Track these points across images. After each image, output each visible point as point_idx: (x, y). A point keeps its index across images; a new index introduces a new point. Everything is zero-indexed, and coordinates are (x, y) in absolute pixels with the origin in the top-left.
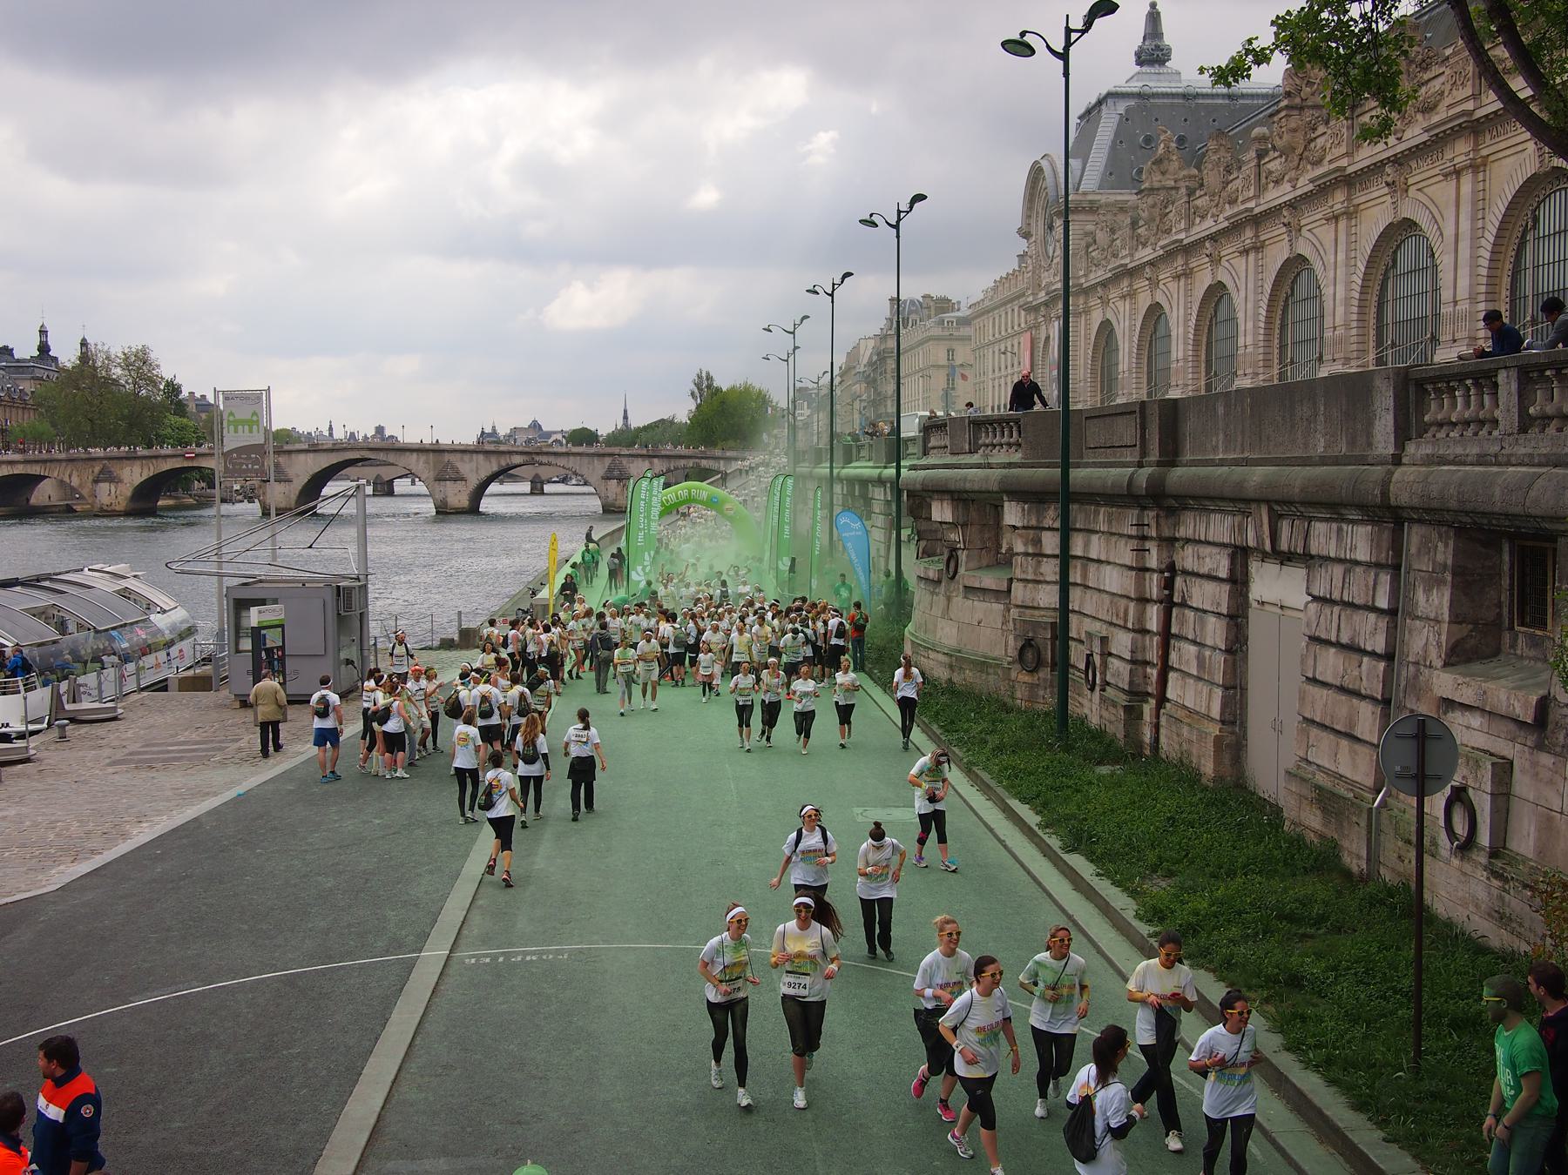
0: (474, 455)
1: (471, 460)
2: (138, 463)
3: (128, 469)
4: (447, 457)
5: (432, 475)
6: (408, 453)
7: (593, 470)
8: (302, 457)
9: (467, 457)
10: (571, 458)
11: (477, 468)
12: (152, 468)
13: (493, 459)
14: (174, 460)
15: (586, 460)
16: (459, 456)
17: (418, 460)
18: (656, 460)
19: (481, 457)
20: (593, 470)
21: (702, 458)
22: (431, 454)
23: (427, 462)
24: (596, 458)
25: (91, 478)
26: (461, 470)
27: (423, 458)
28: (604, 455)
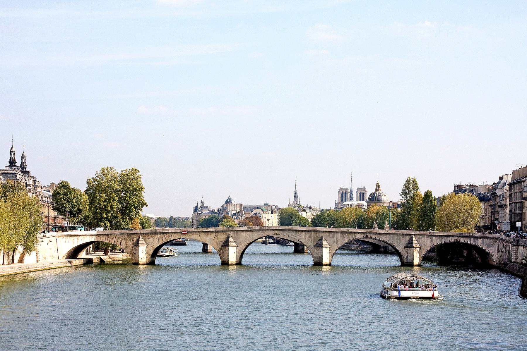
0: (336, 234)
1: (334, 237)
2: (157, 236)
3: (151, 239)
4: (321, 234)
5: (313, 244)
6: (300, 232)
7: (400, 242)
8: (244, 234)
9: (331, 235)
10: (388, 236)
11: (337, 241)
12: (164, 239)
13: (346, 236)
14: (176, 235)
15: (396, 237)
16: (327, 234)
17: (305, 236)
18: (434, 238)
19: (339, 235)
20: (400, 242)
21: (460, 237)
22: (313, 233)
23: (310, 237)
25: (132, 243)
27: (308, 235)
28: (406, 235)
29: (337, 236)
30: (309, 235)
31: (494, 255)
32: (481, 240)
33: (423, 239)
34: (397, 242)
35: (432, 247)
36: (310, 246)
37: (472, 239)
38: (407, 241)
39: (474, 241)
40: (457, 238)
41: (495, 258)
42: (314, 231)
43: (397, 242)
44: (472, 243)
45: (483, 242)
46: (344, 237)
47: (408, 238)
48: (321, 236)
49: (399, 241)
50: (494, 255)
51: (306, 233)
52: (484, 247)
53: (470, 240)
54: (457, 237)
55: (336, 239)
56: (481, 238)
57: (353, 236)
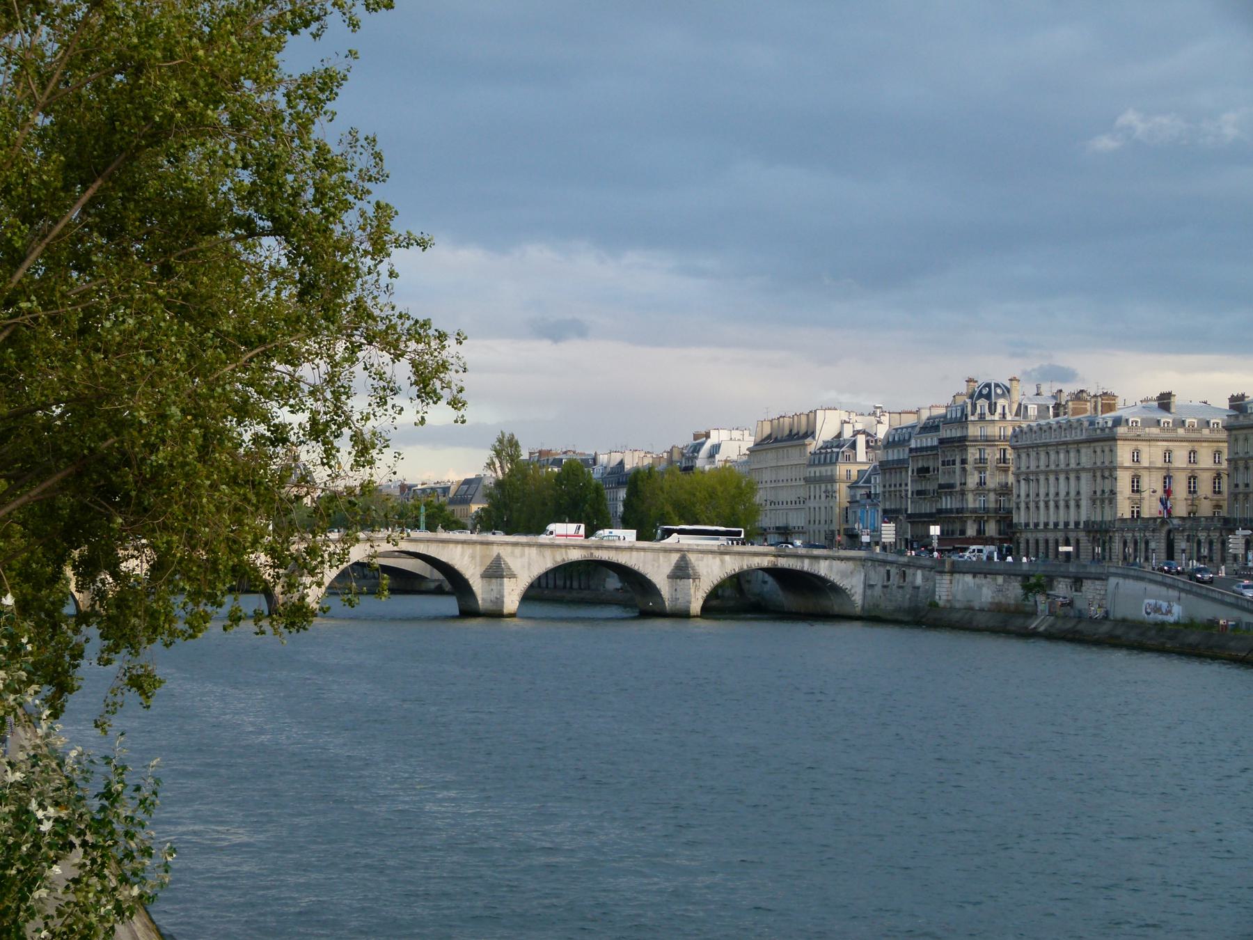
0: (527, 549)
1: (522, 555)
4: (495, 550)
5: (479, 570)
6: (451, 546)
7: (658, 567)
9: (518, 550)
10: (635, 553)
11: (529, 564)
13: (548, 553)
15: (650, 555)
16: (509, 549)
17: (462, 554)
18: (727, 558)
19: (534, 551)
21: (780, 556)
22: (478, 547)
23: (473, 557)
24: (661, 555)
26: (512, 566)
27: (469, 550)
29: (529, 554)
30: (471, 551)
31: (856, 593)
32: (827, 562)
33: (705, 560)
34: (653, 565)
35: (722, 577)
36: (473, 575)
37: (807, 562)
38: (673, 565)
39: (811, 564)
40: (773, 559)
41: (858, 598)
42: (482, 543)
43: (653, 565)
44: (805, 569)
45: (831, 568)
46: (544, 557)
47: (675, 557)
48: (495, 555)
49: (656, 565)
50: (856, 593)
51: (465, 546)
52: (834, 577)
53: (803, 563)
54: (774, 556)
55: (526, 559)
56: (826, 558)
57: (562, 555)
